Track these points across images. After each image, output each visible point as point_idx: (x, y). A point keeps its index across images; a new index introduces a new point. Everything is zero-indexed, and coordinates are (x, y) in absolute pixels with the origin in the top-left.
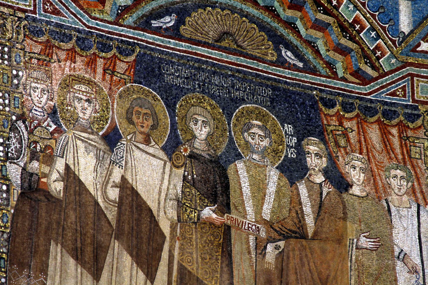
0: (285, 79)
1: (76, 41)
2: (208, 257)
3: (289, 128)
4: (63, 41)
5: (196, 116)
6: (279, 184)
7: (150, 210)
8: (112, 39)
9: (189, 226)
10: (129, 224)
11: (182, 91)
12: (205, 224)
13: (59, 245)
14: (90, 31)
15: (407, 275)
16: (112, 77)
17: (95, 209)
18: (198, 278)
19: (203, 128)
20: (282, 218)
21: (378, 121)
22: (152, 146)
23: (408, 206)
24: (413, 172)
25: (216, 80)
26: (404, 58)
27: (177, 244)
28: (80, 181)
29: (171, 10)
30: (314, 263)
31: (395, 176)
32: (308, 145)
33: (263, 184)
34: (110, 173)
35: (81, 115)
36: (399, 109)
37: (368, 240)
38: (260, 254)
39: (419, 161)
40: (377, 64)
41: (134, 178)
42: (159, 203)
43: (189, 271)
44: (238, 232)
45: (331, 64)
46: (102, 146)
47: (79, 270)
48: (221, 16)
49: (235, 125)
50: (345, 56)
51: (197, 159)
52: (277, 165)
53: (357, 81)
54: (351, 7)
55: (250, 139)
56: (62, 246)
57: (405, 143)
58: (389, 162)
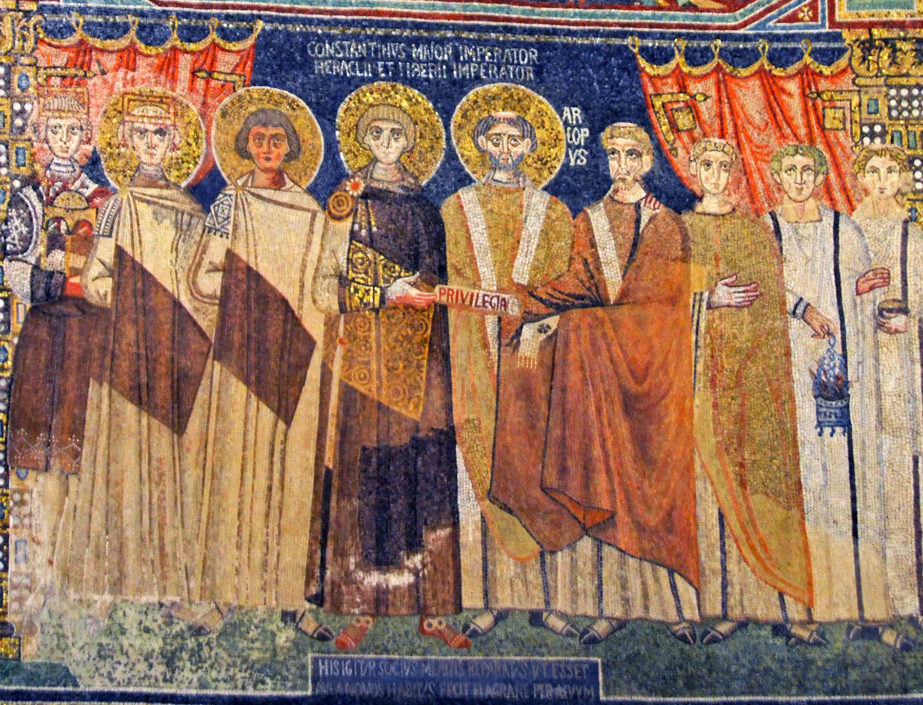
0: (566, 27)
1: (138, 33)
2: (401, 365)
3: (574, 114)
4: (110, 37)
6: (548, 217)
7: (284, 301)
8: (207, 17)
9: (364, 316)
10: (241, 331)
11: (349, 83)
12: (395, 308)
13: (106, 386)
14: (164, 12)
15: (812, 342)
16: (207, 83)
17: (174, 315)
18: (379, 403)
19: (393, 141)
20: (554, 276)
21: (761, 73)
22: (288, 190)
23: (817, 217)
24: (827, 155)
25: (420, 52)
27: (339, 351)
28: (144, 272)
30: (621, 346)
31: (793, 168)
32: (612, 137)
33: (515, 221)
34: (203, 249)
35: (145, 158)
36: (801, 45)
37: (733, 289)
38: (507, 345)
39: (841, 135)
41: (252, 249)
42: (302, 286)
43: (361, 394)
44: (463, 312)
46: (187, 205)
47: (144, 421)
49: (460, 127)
51: (379, 199)
52: (545, 183)
53: (717, 6)
55: (490, 147)
57: (814, 105)
58: (780, 144)
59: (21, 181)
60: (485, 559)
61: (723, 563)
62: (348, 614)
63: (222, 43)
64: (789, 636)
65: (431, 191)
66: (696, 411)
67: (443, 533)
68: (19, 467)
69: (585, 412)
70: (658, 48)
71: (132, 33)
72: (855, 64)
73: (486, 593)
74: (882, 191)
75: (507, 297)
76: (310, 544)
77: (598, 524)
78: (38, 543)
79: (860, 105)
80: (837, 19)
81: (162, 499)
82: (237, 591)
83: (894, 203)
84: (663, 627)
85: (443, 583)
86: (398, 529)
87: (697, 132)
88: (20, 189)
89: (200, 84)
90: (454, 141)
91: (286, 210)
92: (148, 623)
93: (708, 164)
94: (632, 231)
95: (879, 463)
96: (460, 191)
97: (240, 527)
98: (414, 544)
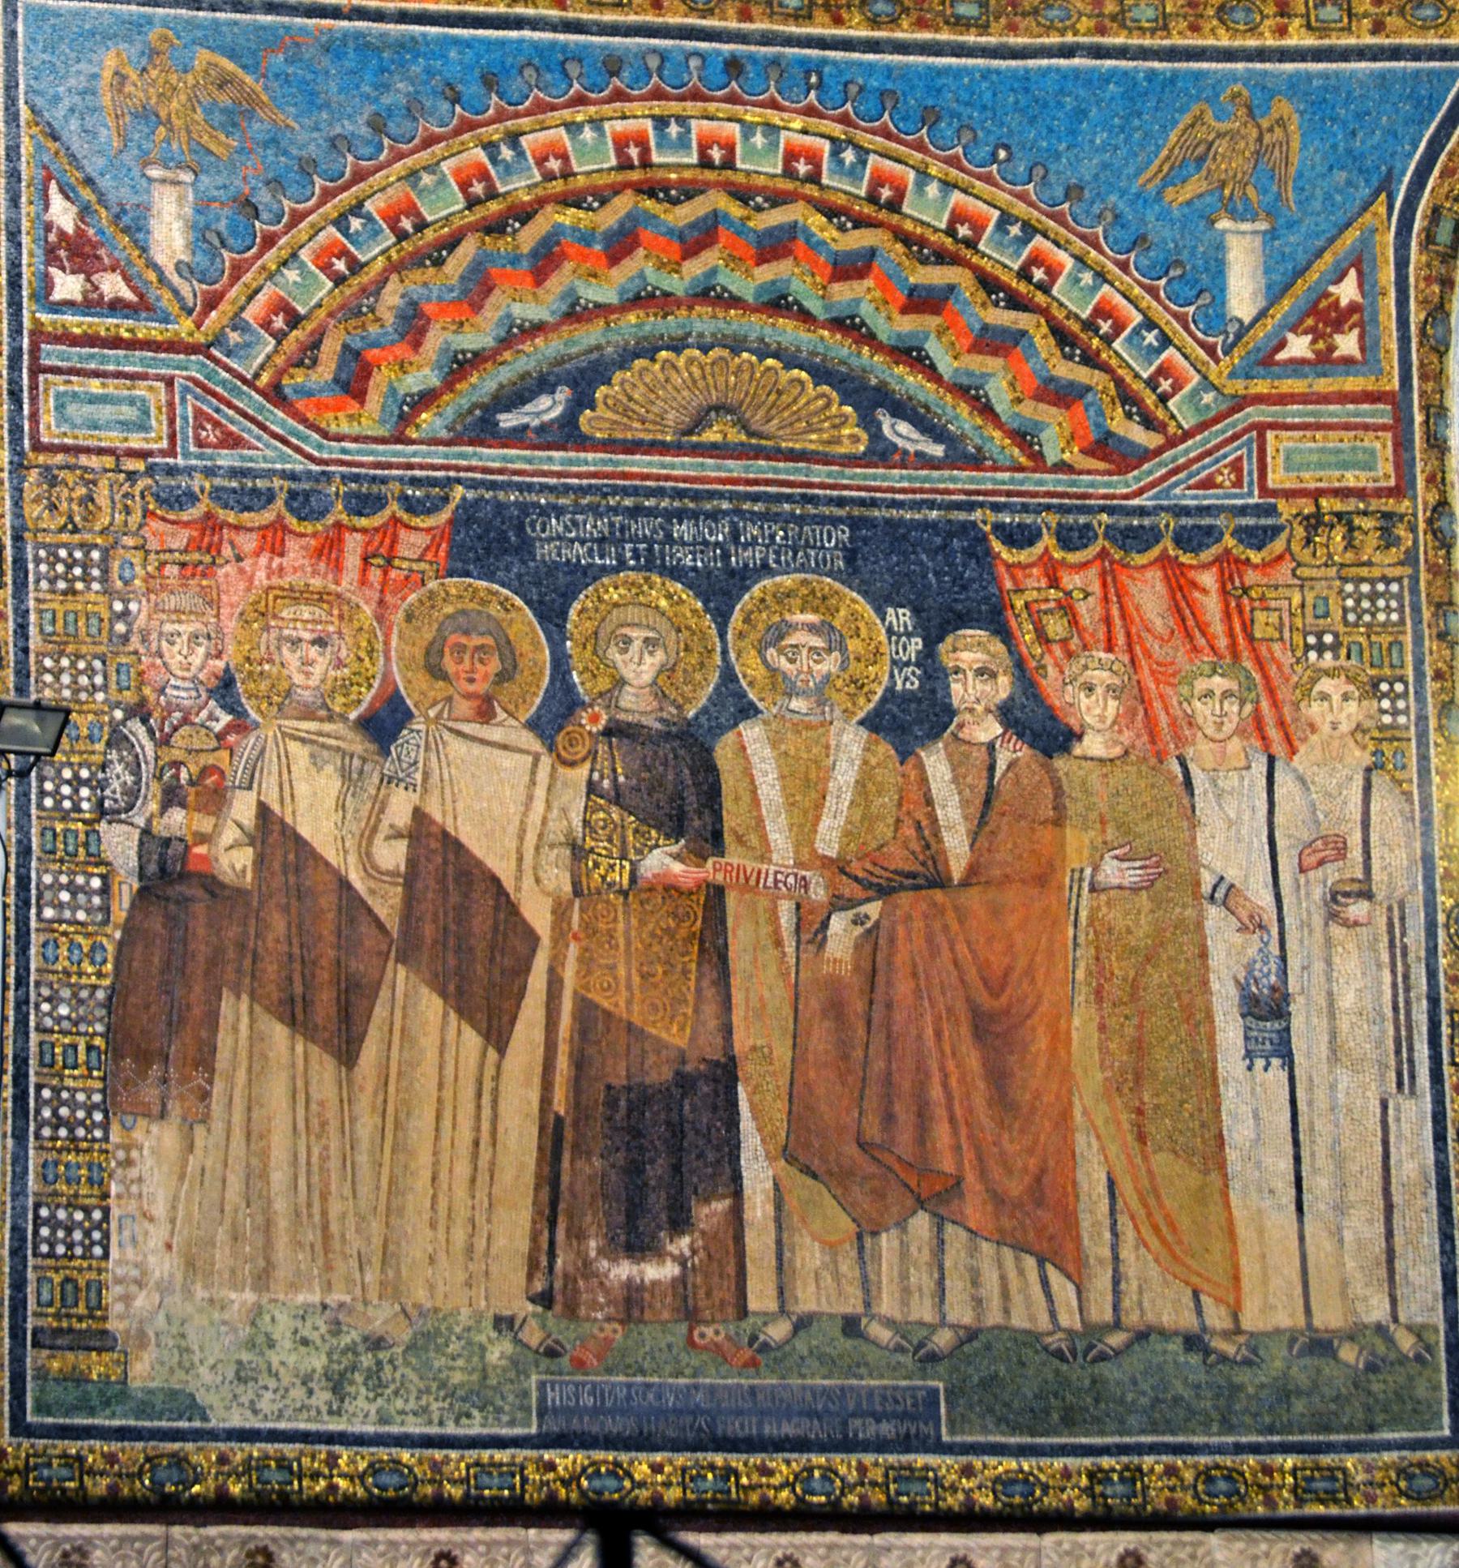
0: (889, 496)
1: (286, 503)
3: (900, 617)
4: (249, 509)
5: (626, 631)
6: (865, 762)
7: (495, 880)
8: (384, 481)
9: (608, 902)
11: (585, 574)
13: (245, 998)
14: (324, 473)
15: (1238, 939)
16: (385, 573)
19: (646, 656)
20: (874, 845)
21: (1164, 561)
23: (1243, 763)
25: (683, 530)
26: (1238, 386)
27: (573, 950)
28: (298, 838)
29: (552, 378)
30: (968, 943)
31: (1209, 694)
32: (955, 650)
33: (819, 768)
34: (380, 806)
35: (298, 679)
36: (1220, 521)
37: (1126, 865)
38: (809, 942)
39: (1276, 647)
40: (1160, 414)
41: (449, 807)
42: (520, 859)
45: (1025, 434)
46: (358, 744)
47: (300, 1048)
48: (702, 368)
49: (741, 635)
50: (1068, 407)
52: (861, 715)
53: (1101, 465)
54: (1087, 278)
55: (783, 663)
56: (253, 997)
58: (1191, 661)
59: (125, 710)
60: (779, 1242)
61: (1115, 1248)
62: (588, 1319)
63: (405, 517)
64: (1207, 1351)
65: (700, 726)
66: (1075, 1035)
67: (721, 1206)
68: (124, 1113)
69: (919, 1037)
70: (1019, 525)
71: (279, 503)
72: (1296, 547)
73: (781, 1292)
74: (1335, 726)
75: (807, 874)
76: (534, 1222)
77: (939, 1194)
78: (151, 1220)
79: (1303, 606)
80: (1270, 484)
81: (324, 1158)
82: (432, 1288)
83: (1352, 744)
84: (1031, 1338)
85: (721, 1276)
86: (657, 1201)
87: (1074, 644)
88: (124, 722)
89: (375, 575)
90: (732, 656)
91: (497, 752)
92: (306, 1332)
93: (1090, 689)
94: (984, 782)
95: (1332, 1109)
96: (741, 726)
97: (434, 1197)
98: (680, 1222)
